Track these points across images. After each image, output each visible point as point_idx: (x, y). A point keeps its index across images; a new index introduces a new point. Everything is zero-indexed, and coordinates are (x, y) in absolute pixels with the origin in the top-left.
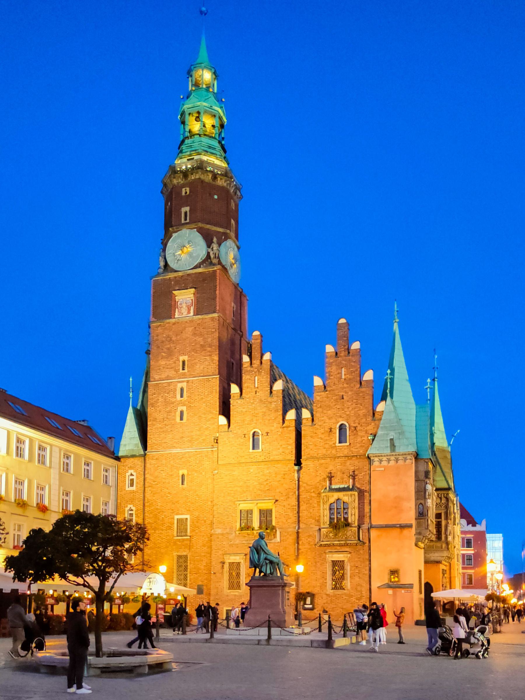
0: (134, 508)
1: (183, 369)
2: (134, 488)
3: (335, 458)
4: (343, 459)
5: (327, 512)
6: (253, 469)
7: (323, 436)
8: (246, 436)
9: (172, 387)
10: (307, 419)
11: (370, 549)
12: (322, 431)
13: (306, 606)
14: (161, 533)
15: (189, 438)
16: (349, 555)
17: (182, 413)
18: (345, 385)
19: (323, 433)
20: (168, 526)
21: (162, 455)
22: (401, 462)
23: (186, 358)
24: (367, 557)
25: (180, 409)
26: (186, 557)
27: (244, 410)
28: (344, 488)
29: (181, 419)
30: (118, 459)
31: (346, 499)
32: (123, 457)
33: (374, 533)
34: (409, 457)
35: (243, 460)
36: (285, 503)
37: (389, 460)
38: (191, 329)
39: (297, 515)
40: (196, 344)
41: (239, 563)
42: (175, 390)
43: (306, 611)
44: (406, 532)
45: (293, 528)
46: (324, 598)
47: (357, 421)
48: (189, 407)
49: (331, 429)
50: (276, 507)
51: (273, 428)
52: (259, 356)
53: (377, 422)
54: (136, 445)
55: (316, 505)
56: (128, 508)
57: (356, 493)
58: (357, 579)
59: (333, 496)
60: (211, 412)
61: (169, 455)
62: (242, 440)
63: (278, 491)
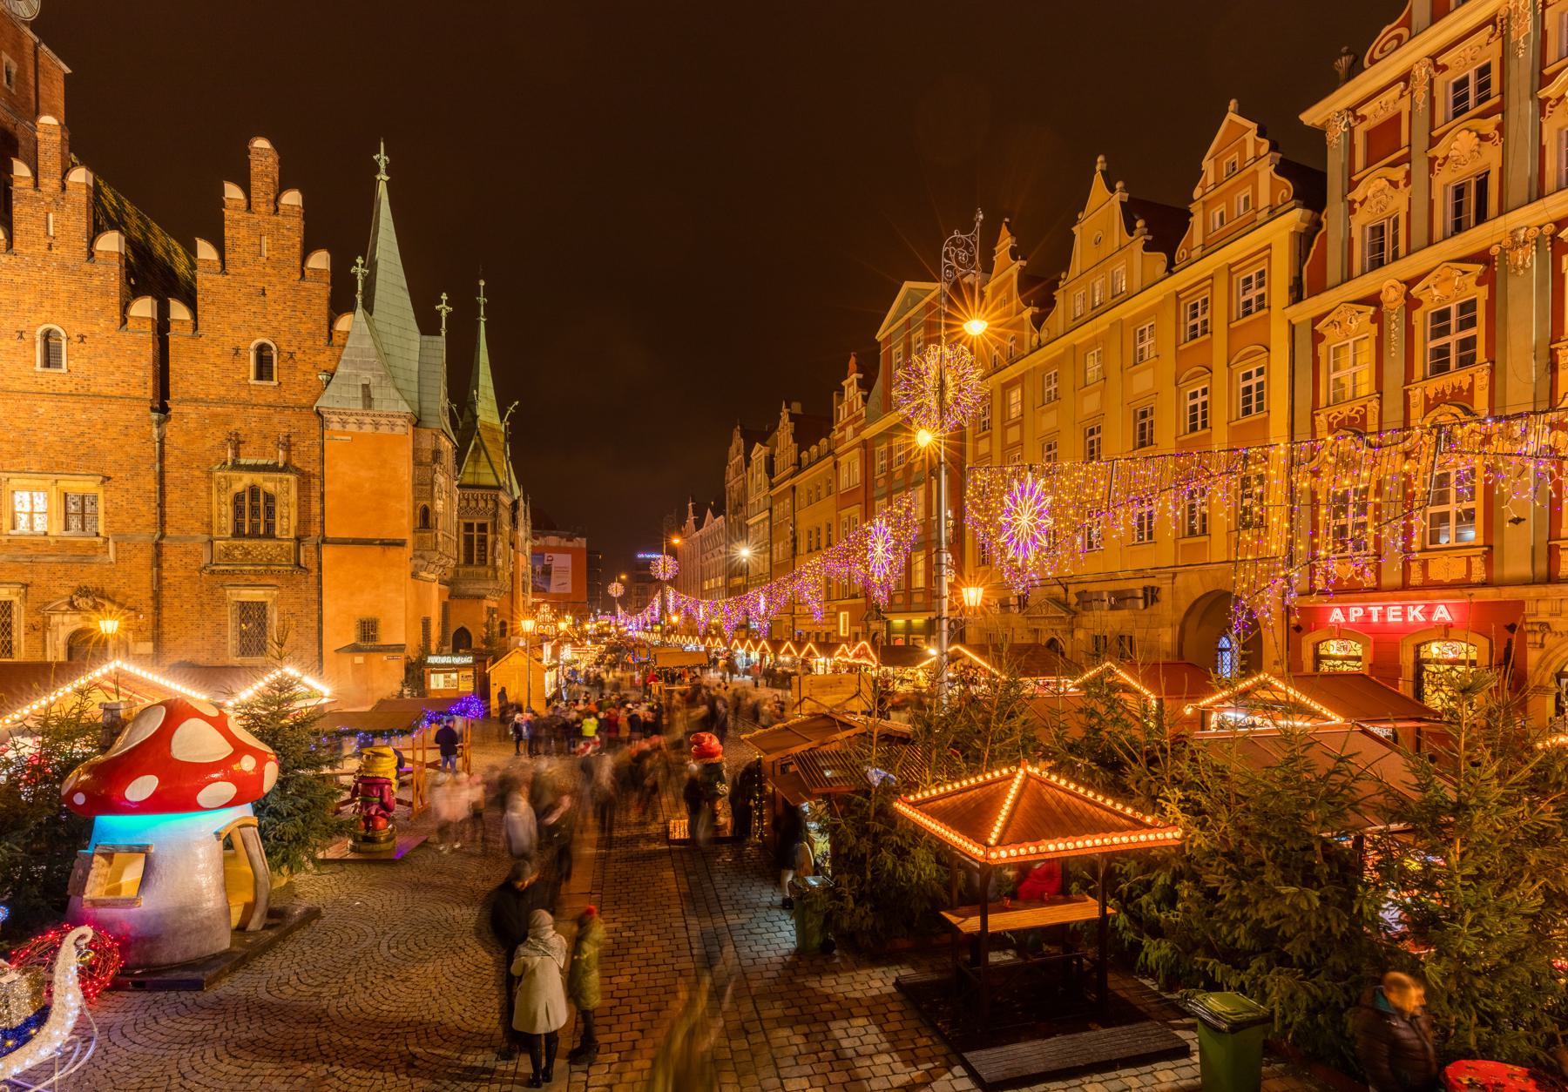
3: (246, 404)
4: (265, 410)
5: (228, 510)
6: (44, 408)
7: (219, 362)
10: (183, 322)
11: (320, 583)
12: (218, 350)
18: (268, 270)
22: (384, 430)
24: (315, 596)
27: (19, 280)
31: (269, 487)
33: (328, 553)
34: (400, 422)
35: (17, 386)
36: (129, 485)
37: (360, 424)
44: (393, 553)
45: (148, 534)
47: (295, 343)
49: (237, 351)
51: (96, 329)
52: (58, 170)
55: (204, 494)
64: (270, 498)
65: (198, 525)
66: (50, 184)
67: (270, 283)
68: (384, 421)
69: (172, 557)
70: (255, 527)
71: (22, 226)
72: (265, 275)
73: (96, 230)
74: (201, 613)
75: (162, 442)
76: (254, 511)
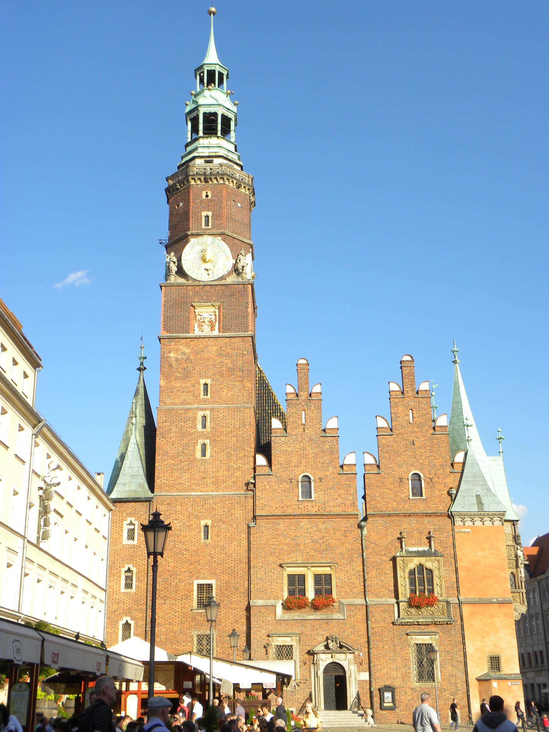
0: (134, 569)
7: (392, 487)
8: (293, 481)
9: (190, 414)
11: (463, 629)
14: (173, 604)
15: (214, 480)
16: (437, 637)
18: (416, 429)
19: (391, 484)
20: (185, 595)
23: (209, 381)
24: (461, 639)
25: (200, 442)
27: (290, 449)
28: (424, 551)
29: (204, 454)
33: (466, 609)
35: (290, 511)
38: (215, 348)
40: (221, 366)
42: (195, 419)
43: (384, 712)
46: (408, 694)
47: (433, 472)
48: (213, 441)
49: (401, 480)
50: (336, 572)
51: (328, 474)
54: (140, 485)
58: (449, 668)
59: (412, 561)
61: (186, 500)
62: (288, 486)
63: (338, 551)
64: (430, 571)
66: (304, 395)
67: (416, 437)
70: (422, 592)
71: (291, 420)
72: (413, 432)
74: (395, 651)
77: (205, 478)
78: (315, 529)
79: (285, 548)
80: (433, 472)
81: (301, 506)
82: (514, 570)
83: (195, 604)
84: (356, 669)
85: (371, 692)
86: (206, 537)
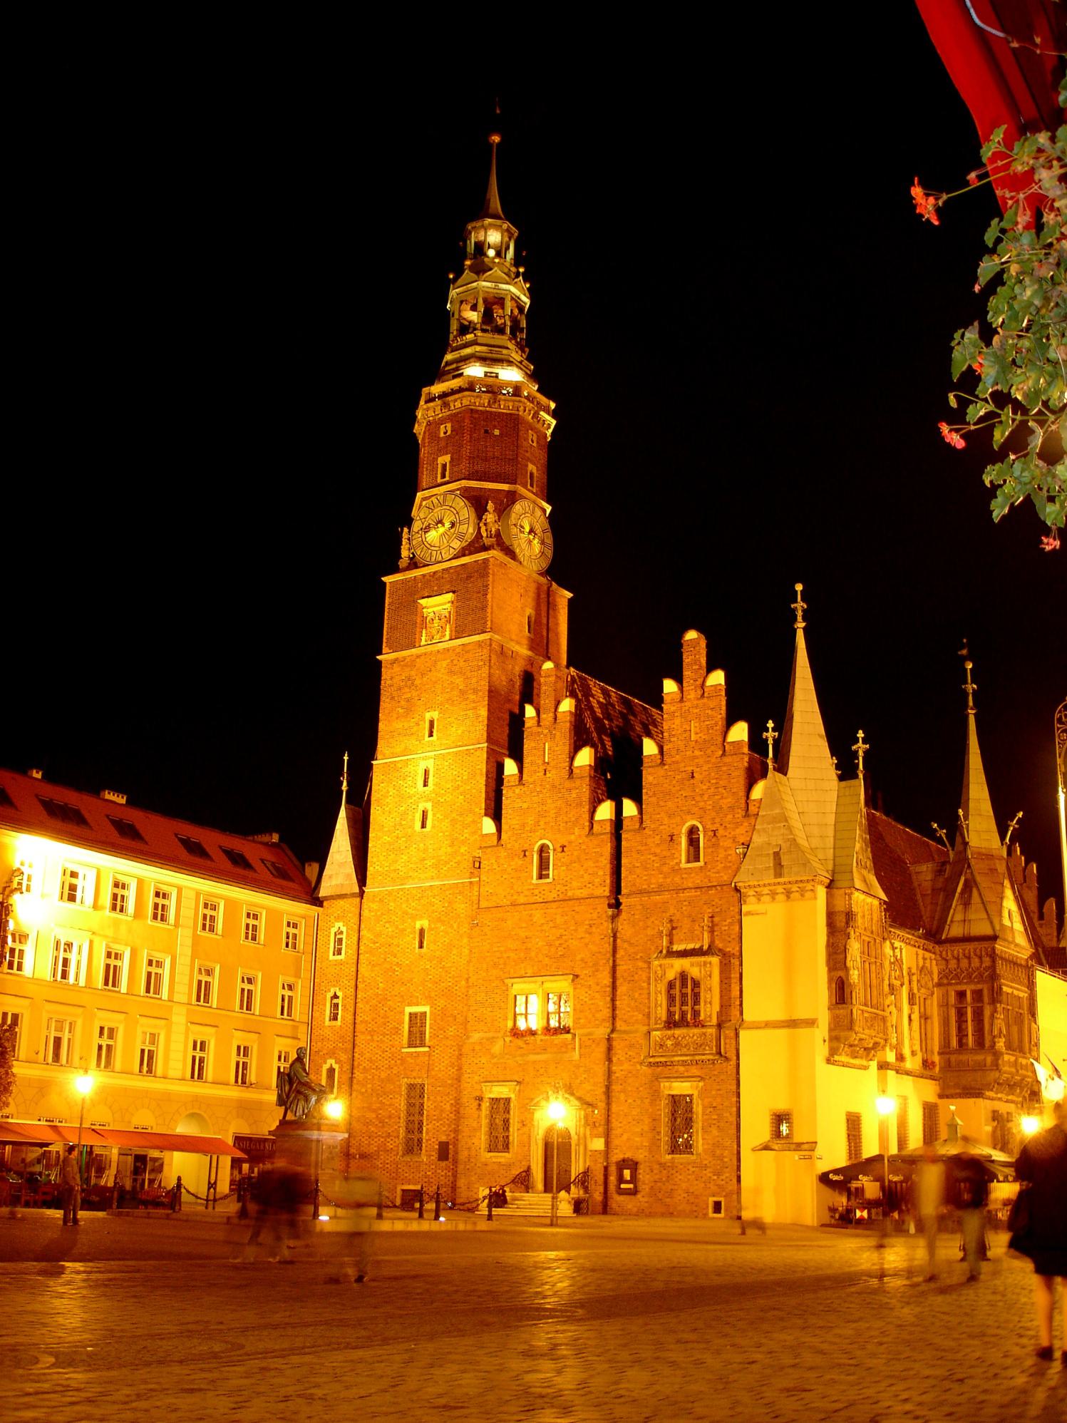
0: (339, 994)
1: (431, 735)
2: (342, 957)
4: (693, 893)
5: (662, 999)
6: (538, 915)
7: (658, 851)
10: (632, 817)
13: (623, 1186)
14: (382, 1041)
16: (701, 1084)
17: (424, 814)
18: (697, 753)
21: (390, 893)
23: (435, 715)
25: (421, 808)
26: (422, 1086)
27: (525, 806)
29: (423, 826)
30: (318, 902)
31: (695, 972)
32: (327, 898)
35: (522, 899)
38: (444, 664)
39: (609, 1005)
41: (508, 1100)
43: (622, 1198)
47: (717, 820)
48: (436, 804)
49: (672, 836)
53: (752, 820)
54: (348, 875)
55: (645, 985)
56: (332, 994)
57: (715, 960)
58: (715, 1132)
60: (471, 811)
63: (579, 957)
64: (696, 984)
65: (640, 1016)
68: (795, 888)
69: (619, 1053)
70: (683, 1014)
73: (576, 749)
75: (615, 937)
76: (684, 995)
77: (424, 859)
78: (551, 924)
79: (512, 955)
80: (717, 820)
81: (536, 892)
82: (841, 973)
83: (405, 1041)
84: (588, 1133)
85: (606, 1168)
86: (421, 946)
